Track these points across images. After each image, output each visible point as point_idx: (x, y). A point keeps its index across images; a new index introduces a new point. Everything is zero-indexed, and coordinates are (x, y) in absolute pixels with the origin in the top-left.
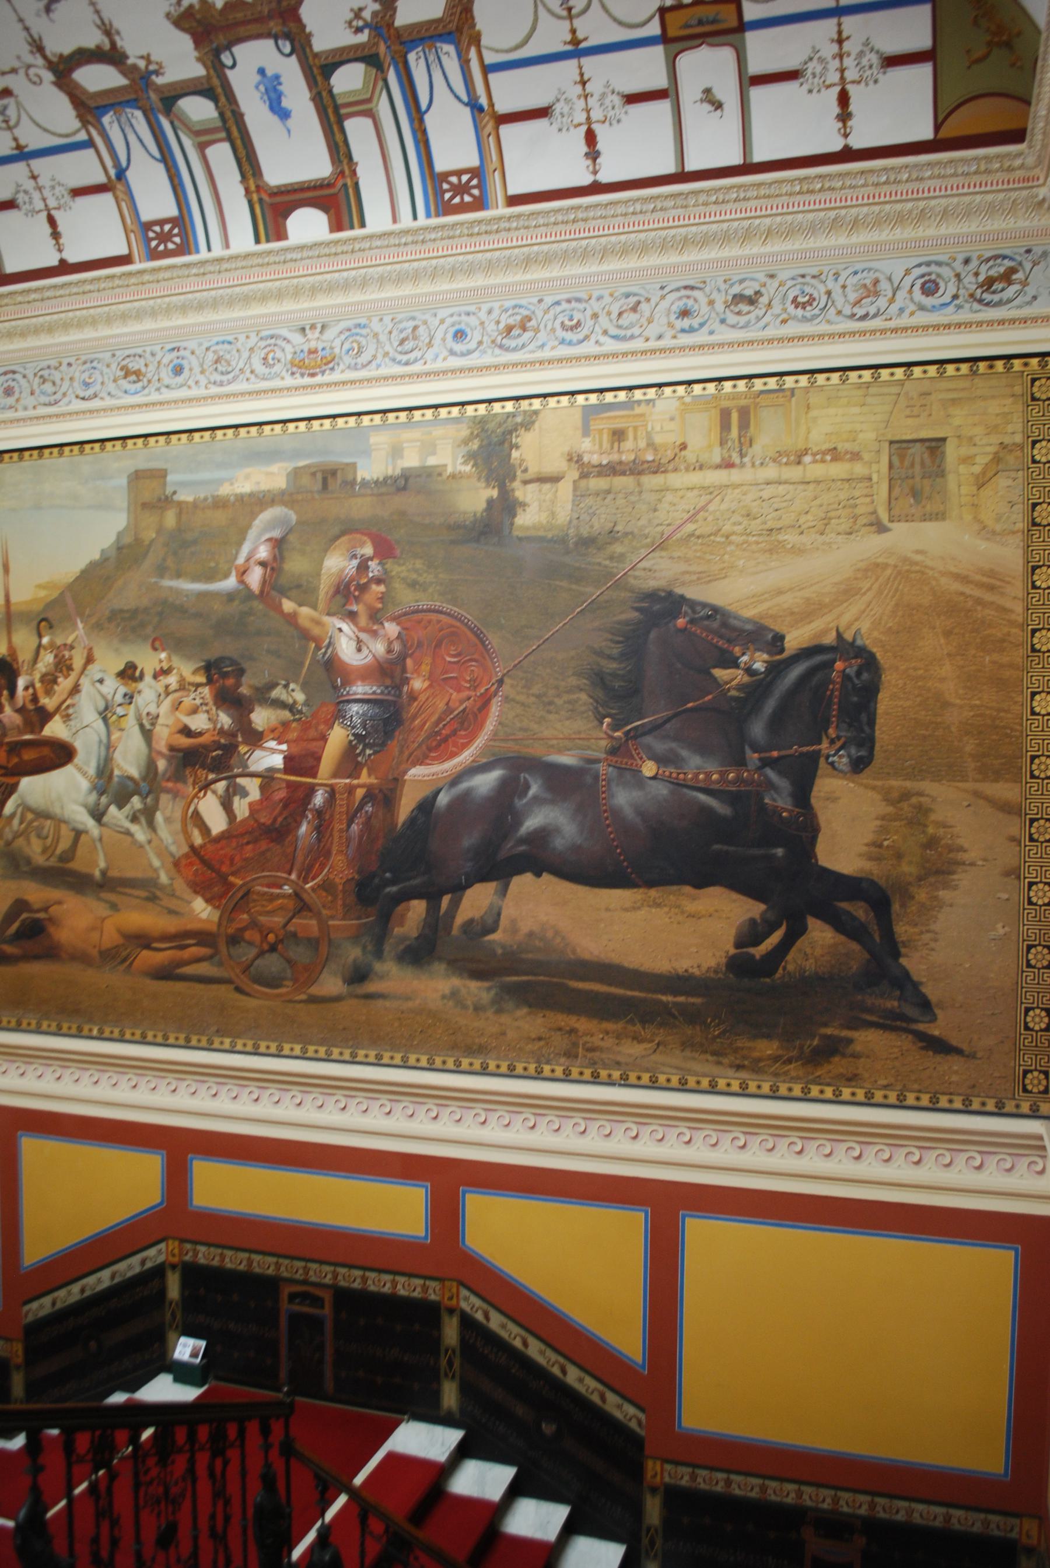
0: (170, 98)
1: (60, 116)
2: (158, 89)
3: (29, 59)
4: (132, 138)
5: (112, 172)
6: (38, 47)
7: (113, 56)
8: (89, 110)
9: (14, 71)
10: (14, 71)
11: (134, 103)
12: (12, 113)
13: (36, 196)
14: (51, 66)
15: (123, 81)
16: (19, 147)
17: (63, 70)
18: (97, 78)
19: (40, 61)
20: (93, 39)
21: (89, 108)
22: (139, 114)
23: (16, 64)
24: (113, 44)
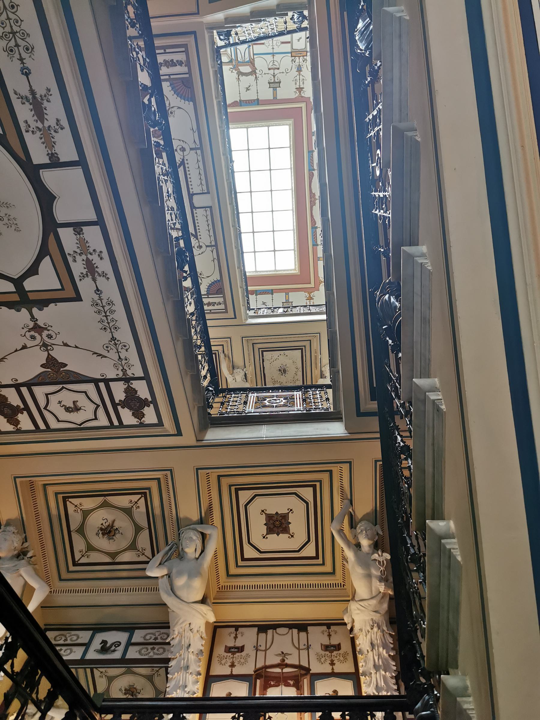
0: (231, 61)
1: (258, 62)
2: (232, 65)
3: (260, 76)
4: (243, 55)
5: (251, 47)
6: (256, 78)
7: (240, 73)
8: (251, 62)
9: (265, 74)
10: (265, 74)
11: (239, 62)
12: (271, 64)
13: (274, 44)
14: (255, 73)
15: (239, 67)
16: (273, 56)
17: (254, 72)
18: (246, 69)
19: (257, 75)
20: (242, 78)
21: (252, 63)
22: (239, 60)
23: (264, 75)
24: (239, 76)
